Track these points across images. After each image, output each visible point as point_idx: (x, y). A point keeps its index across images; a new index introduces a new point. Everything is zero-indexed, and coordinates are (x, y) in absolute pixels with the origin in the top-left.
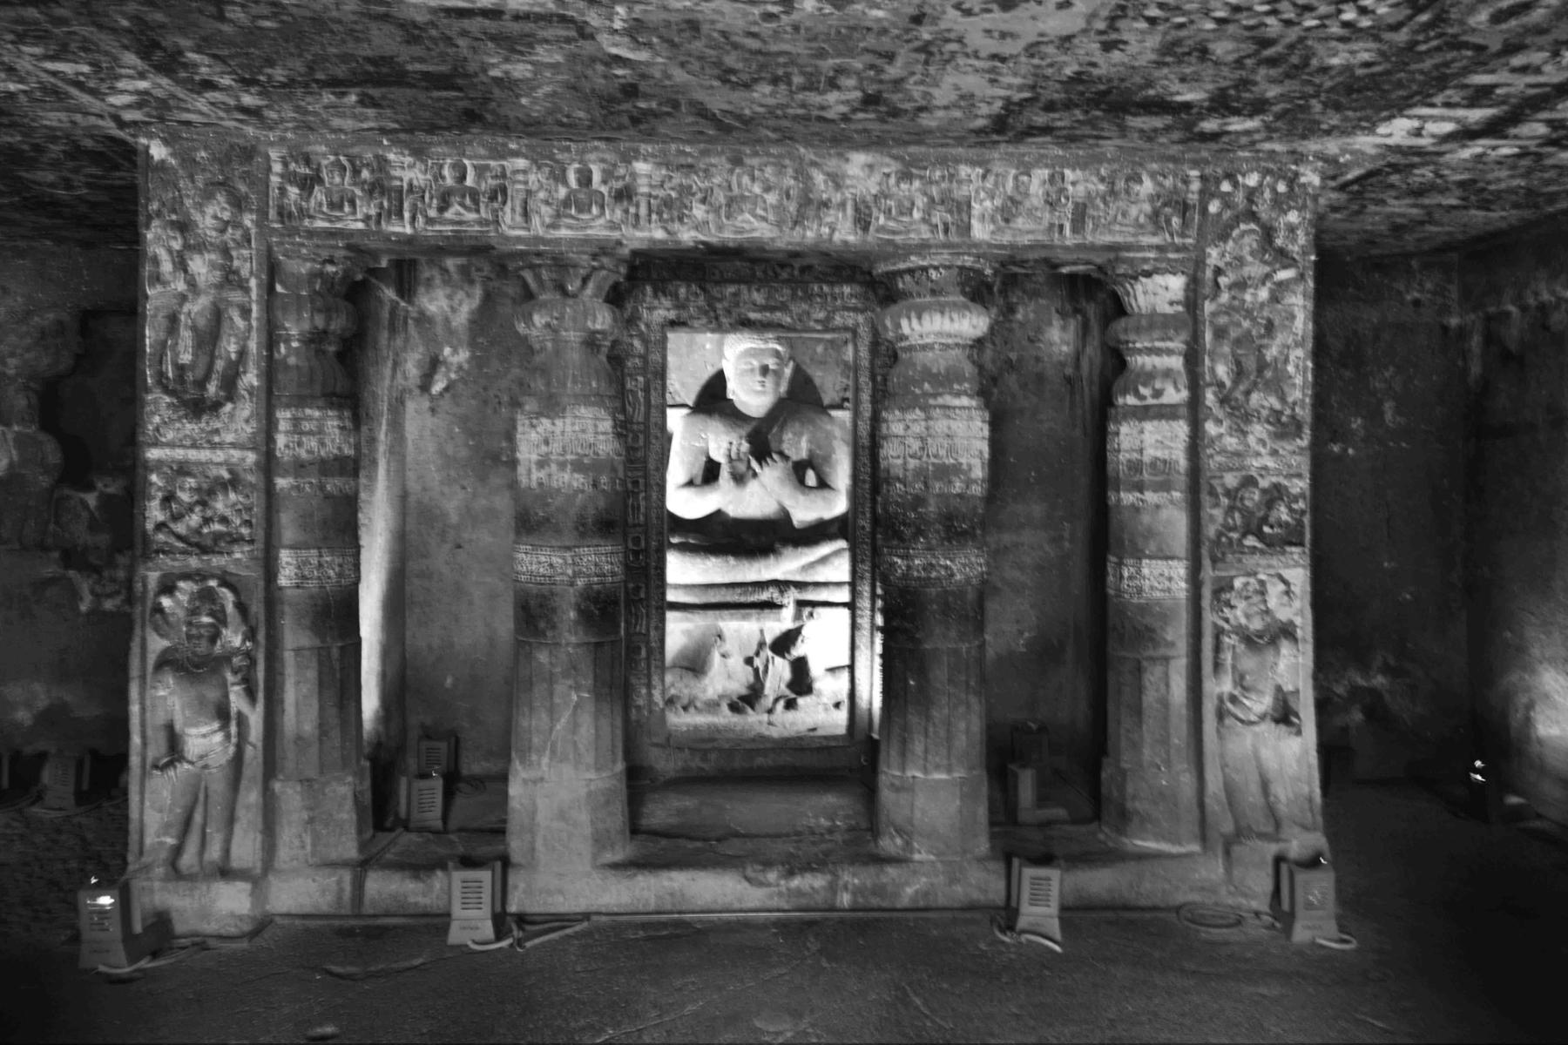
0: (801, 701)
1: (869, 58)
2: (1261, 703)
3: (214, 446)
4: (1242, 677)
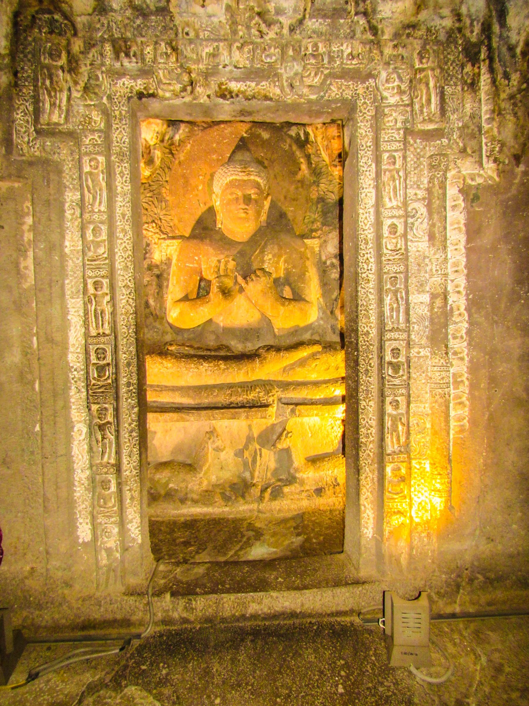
0: (286, 490)
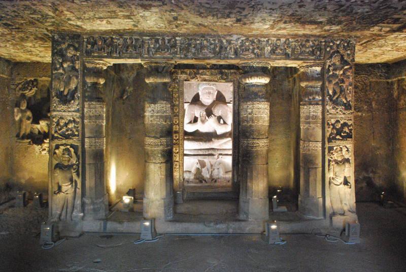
1: (238, 9)
2: (341, 180)
3: (69, 111)
4: (335, 173)
